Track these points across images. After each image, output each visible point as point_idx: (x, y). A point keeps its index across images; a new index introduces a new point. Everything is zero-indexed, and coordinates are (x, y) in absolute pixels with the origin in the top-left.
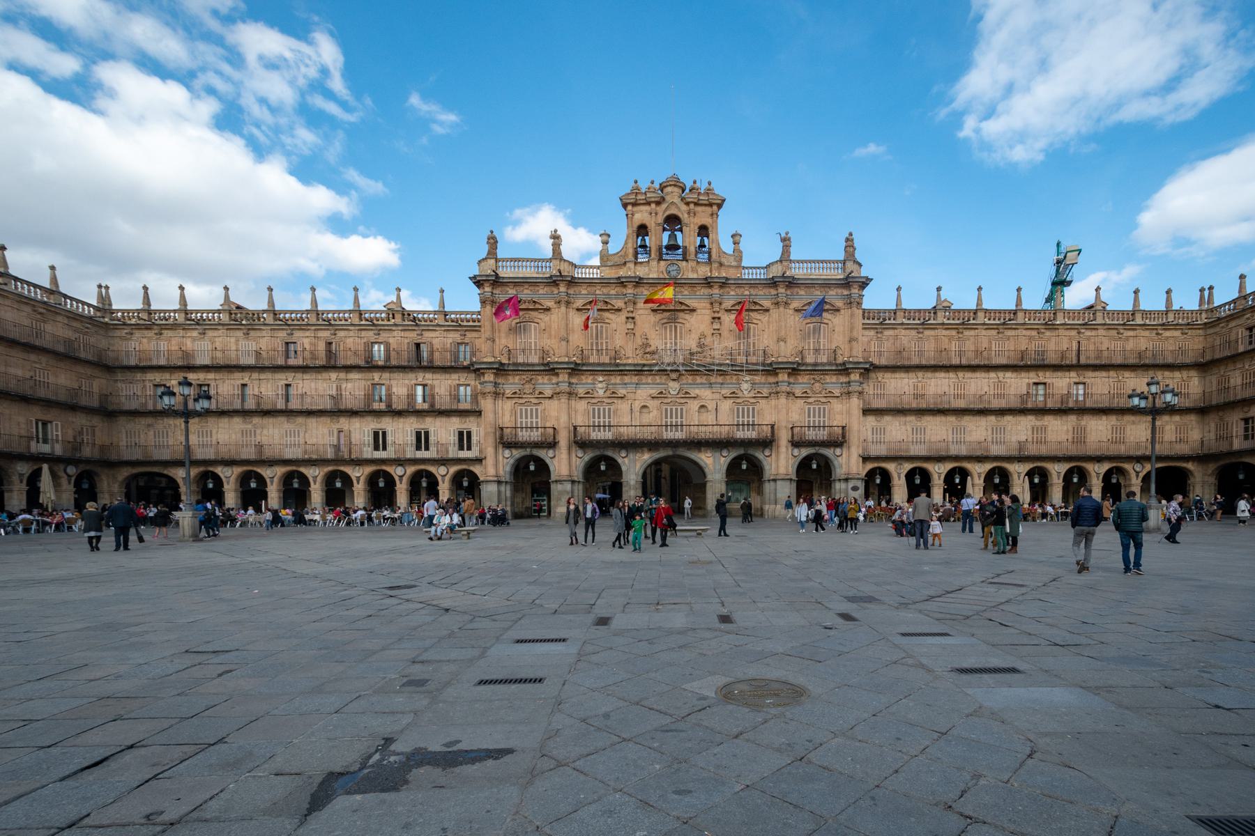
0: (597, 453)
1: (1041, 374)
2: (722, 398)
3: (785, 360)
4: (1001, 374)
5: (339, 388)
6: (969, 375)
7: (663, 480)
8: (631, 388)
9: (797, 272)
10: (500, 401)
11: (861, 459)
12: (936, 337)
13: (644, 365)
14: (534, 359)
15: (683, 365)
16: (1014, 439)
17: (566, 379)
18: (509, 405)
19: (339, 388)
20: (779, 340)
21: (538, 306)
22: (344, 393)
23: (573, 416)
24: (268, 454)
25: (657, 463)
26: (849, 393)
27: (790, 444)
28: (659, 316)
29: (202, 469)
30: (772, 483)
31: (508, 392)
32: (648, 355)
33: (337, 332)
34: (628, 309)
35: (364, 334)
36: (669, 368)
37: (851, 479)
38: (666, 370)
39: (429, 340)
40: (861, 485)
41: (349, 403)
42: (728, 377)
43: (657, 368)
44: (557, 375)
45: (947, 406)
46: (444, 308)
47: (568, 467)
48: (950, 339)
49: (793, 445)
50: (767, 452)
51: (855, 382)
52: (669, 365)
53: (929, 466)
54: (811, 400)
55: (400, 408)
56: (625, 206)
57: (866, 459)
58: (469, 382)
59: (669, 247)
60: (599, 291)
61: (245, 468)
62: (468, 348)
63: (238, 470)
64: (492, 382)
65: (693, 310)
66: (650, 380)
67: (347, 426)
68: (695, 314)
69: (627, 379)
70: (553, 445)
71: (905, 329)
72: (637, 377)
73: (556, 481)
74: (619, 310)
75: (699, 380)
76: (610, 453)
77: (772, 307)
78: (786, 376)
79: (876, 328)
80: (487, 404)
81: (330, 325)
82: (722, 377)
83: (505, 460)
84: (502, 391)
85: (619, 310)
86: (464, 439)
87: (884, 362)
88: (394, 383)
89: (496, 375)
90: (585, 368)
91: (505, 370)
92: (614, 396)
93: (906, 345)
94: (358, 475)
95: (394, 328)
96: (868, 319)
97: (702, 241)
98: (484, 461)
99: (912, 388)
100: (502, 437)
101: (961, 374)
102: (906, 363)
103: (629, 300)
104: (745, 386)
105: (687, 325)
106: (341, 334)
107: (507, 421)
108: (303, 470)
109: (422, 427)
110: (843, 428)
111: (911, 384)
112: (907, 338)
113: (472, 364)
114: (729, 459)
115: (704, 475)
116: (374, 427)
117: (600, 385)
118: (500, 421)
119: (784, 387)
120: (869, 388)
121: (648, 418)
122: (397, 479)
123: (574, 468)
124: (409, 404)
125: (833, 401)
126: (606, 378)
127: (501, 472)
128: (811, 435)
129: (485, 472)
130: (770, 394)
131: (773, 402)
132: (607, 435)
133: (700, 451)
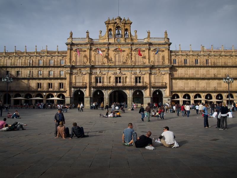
1: (219, 68)
4: (208, 68)
6: (199, 68)
7: (116, 97)
16: (213, 86)
21: (82, 50)
24: (12, 89)
28: (114, 52)
54: (156, 75)
56: (106, 24)
59: (117, 34)
65: (124, 51)
70: (86, 87)
74: (104, 51)
75: (125, 69)
76: (100, 90)
85: (104, 51)
94: (34, 95)
97: (126, 32)
101: (197, 68)
115: (127, 96)
117: (98, 71)
129: (67, 95)
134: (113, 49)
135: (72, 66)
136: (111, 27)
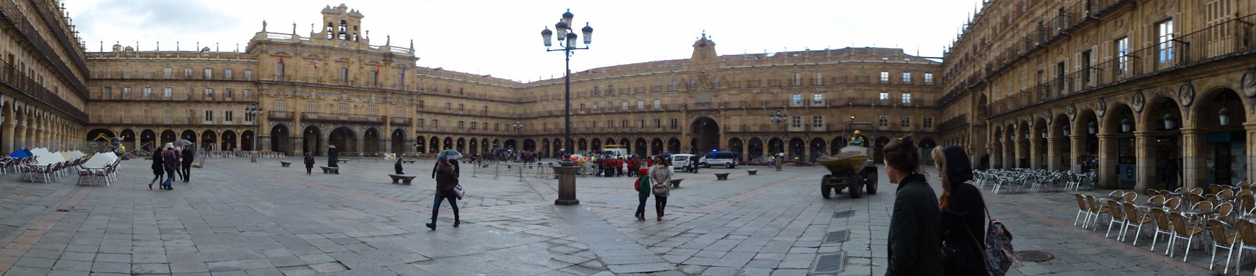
0: (310, 124)
8: (326, 95)
9: (392, 50)
20: (386, 79)
24: (159, 121)
28: (339, 64)
29: (126, 128)
30: (383, 143)
40: (416, 143)
50: (381, 128)
57: (417, 132)
60: (313, 51)
61: (145, 128)
63: (143, 129)
66: (334, 92)
69: (324, 91)
73: (294, 138)
76: (316, 125)
92: (318, 98)
108: (173, 130)
134: (337, 58)
136: (330, 19)
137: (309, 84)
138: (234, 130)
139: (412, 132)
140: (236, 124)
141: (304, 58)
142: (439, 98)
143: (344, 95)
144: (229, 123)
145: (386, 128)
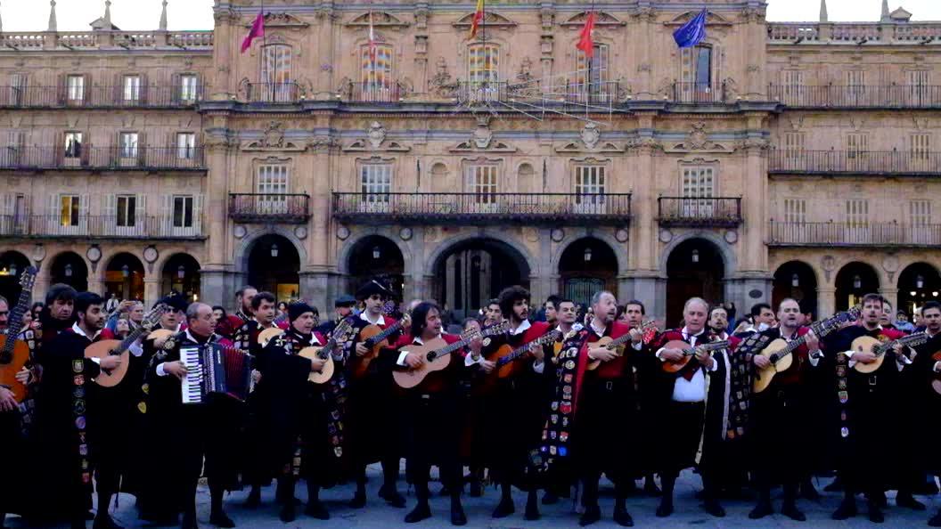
0: (369, 232)
2: (553, 153)
3: (648, 98)
5: (22, 138)
10: (233, 157)
11: (766, 249)
12: (881, 67)
13: (439, 105)
14: (284, 96)
15: (495, 104)
17: (327, 125)
18: (246, 161)
19: (22, 138)
21: (291, 23)
22: (28, 145)
23: (335, 178)
25: (455, 249)
26: (746, 148)
27: (656, 224)
31: (245, 145)
32: (446, 91)
33: (25, 61)
34: (418, 25)
35: (59, 63)
36: (475, 109)
37: (749, 279)
38: (471, 112)
39: (144, 70)
41: (33, 158)
42: (563, 122)
43: (456, 109)
44: (314, 118)
45: (902, 170)
46: (165, 26)
47: (325, 250)
48: (902, 69)
49: (660, 225)
50: (622, 234)
51: (755, 131)
52: (474, 105)
53: (875, 261)
54: (688, 158)
55: (98, 165)
57: (773, 248)
58: (193, 129)
62: (194, 80)
64: (220, 129)
65: (514, 26)
66: (447, 126)
67: (30, 190)
68: (516, 30)
69: (415, 125)
70: (304, 219)
71: (833, 53)
72: (428, 122)
73: (306, 274)
74: (406, 26)
75: (520, 126)
76: (386, 232)
77: (629, 21)
78: (650, 122)
79: (790, 52)
80: (215, 161)
81: (17, 51)
82: (554, 123)
83: (237, 241)
84: (236, 142)
85: (406, 26)
86: (183, 211)
87: (802, 101)
88: (93, 130)
89: (229, 119)
90: (353, 109)
91: (242, 112)
93: (836, 77)
94: (39, 259)
95: (98, 55)
96: (777, 38)
98: (207, 242)
99: (845, 141)
100: (232, 209)
101: (920, 122)
102: (836, 104)
103: (421, 13)
104: (589, 137)
105: (505, 47)
106: (30, 63)
107: (241, 185)
109: (127, 192)
110: (739, 200)
111: (843, 135)
112: (836, 69)
113: (197, 104)
114: (563, 246)
116: (63, 191)
117: (375, 134)
118: (232, 184)
119: (647, 139)
120: (781, 138)
121: (449, 181)
122: (89, 265)
123: (333, 254)
124: (111, 159)
125: (724, 160)
126: (384, 123)
127: (230, 258)
128: (689, 211)
130: (627, 148)
131: (631, 160)
132: (383, 207)
133: (519, 232)
134: (456, 16)
135: (237, 104)
137: (361, 104)
138: (137, 252)
139: (746, 242)
140: (141, 233)
141: (348, 26)
142: (871, 120)
143: (480, 133)
144: (125, 231)
145: (637, 237)
